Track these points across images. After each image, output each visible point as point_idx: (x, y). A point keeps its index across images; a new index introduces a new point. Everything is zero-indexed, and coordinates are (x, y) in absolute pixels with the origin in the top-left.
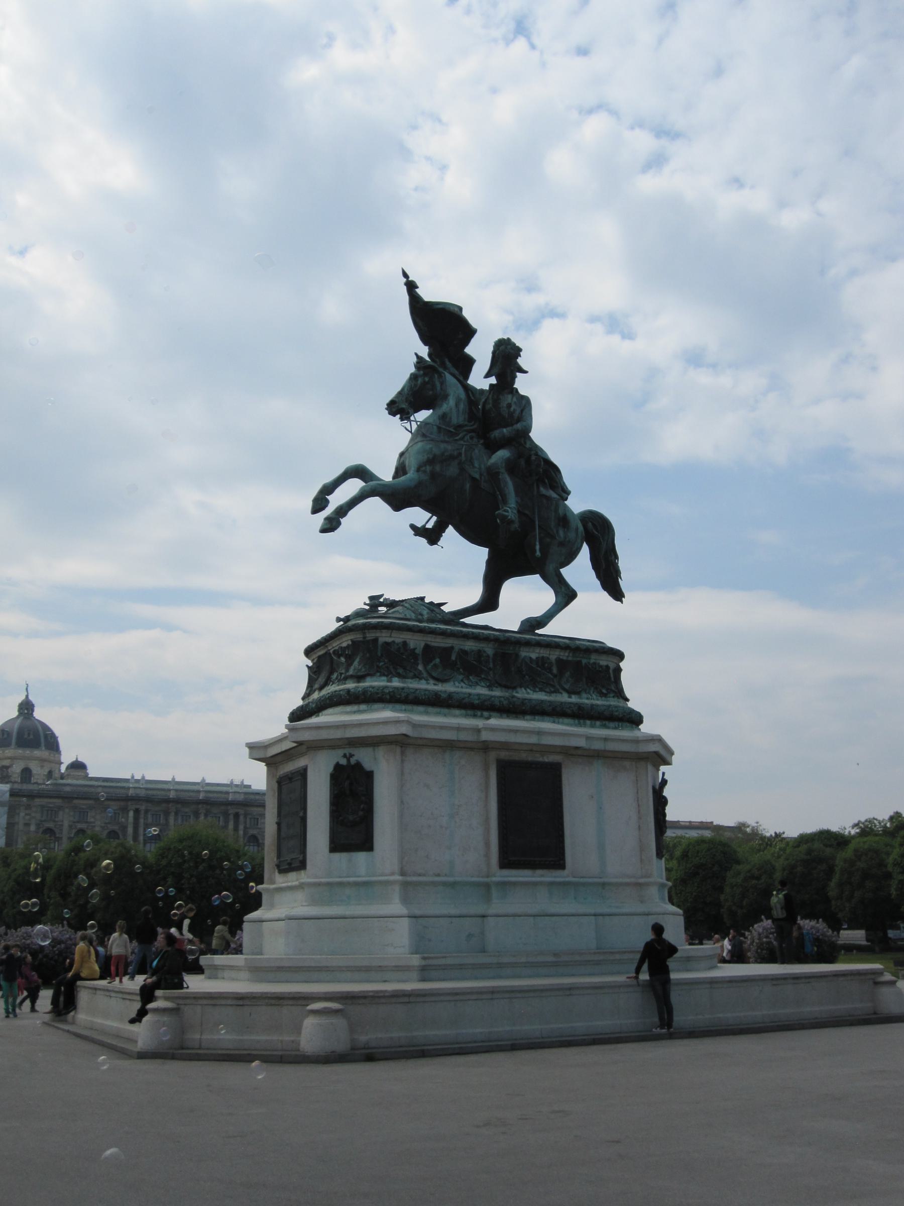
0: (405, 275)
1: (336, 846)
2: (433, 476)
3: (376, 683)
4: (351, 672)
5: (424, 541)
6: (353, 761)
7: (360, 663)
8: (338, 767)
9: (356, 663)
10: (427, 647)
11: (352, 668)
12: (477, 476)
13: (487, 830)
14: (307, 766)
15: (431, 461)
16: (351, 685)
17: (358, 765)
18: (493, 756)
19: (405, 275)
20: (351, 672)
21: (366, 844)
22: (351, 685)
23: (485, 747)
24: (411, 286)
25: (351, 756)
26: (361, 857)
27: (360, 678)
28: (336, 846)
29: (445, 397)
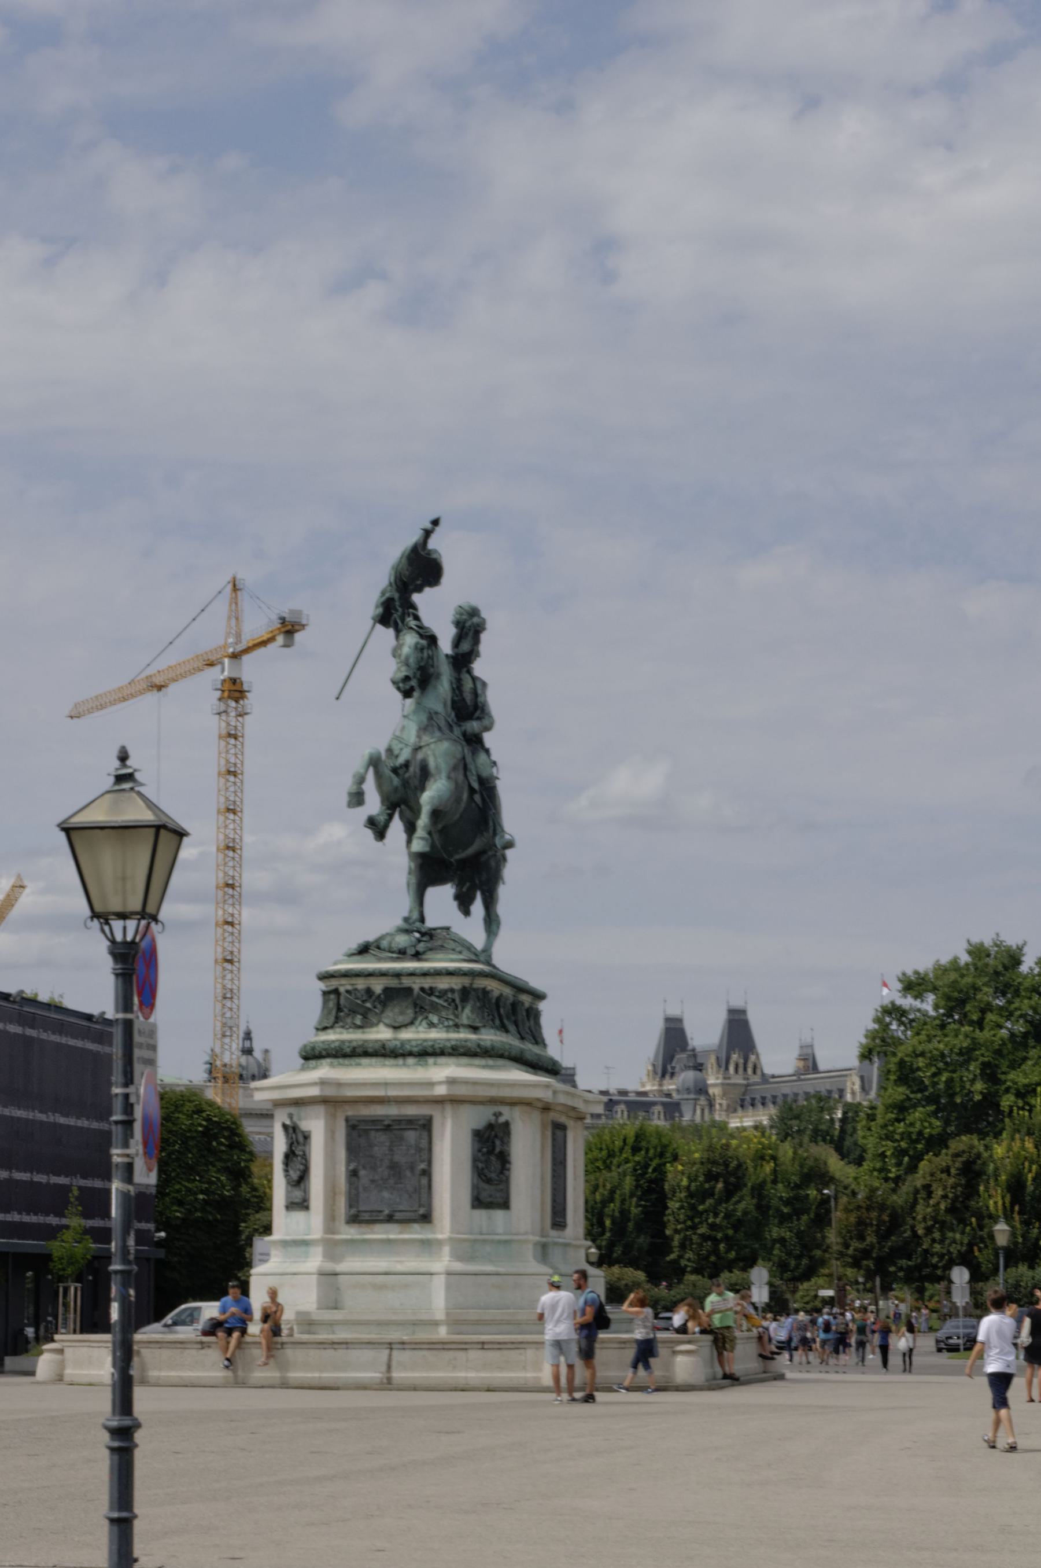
0: (436, 522)
1: (479, 1202)
2: (456, 783)
3: (489, 1037)
4: (464, 1020)
5: (369, 833)
6: (502, 1120)
7: (472, 1011)
8: (490, 1126)
9: (467, 1011)
10: (501, 995)
11: (464, 1016)
12: (476, 785)
13: (543, 1192)
15: (455, 768)
16: (464, 1035)
17: (507, 1124)
18: (552, 1115)
19: (436, 522)
20: (465, 1021)
21: (505, 1204)
22: (464, 1035)
23: (546, 1108)
24: (428, 533)
25: (500, 1114)
26: (499, 1214)
27: (475, 1029)
28: (479, 1202)
29: (438, 676)
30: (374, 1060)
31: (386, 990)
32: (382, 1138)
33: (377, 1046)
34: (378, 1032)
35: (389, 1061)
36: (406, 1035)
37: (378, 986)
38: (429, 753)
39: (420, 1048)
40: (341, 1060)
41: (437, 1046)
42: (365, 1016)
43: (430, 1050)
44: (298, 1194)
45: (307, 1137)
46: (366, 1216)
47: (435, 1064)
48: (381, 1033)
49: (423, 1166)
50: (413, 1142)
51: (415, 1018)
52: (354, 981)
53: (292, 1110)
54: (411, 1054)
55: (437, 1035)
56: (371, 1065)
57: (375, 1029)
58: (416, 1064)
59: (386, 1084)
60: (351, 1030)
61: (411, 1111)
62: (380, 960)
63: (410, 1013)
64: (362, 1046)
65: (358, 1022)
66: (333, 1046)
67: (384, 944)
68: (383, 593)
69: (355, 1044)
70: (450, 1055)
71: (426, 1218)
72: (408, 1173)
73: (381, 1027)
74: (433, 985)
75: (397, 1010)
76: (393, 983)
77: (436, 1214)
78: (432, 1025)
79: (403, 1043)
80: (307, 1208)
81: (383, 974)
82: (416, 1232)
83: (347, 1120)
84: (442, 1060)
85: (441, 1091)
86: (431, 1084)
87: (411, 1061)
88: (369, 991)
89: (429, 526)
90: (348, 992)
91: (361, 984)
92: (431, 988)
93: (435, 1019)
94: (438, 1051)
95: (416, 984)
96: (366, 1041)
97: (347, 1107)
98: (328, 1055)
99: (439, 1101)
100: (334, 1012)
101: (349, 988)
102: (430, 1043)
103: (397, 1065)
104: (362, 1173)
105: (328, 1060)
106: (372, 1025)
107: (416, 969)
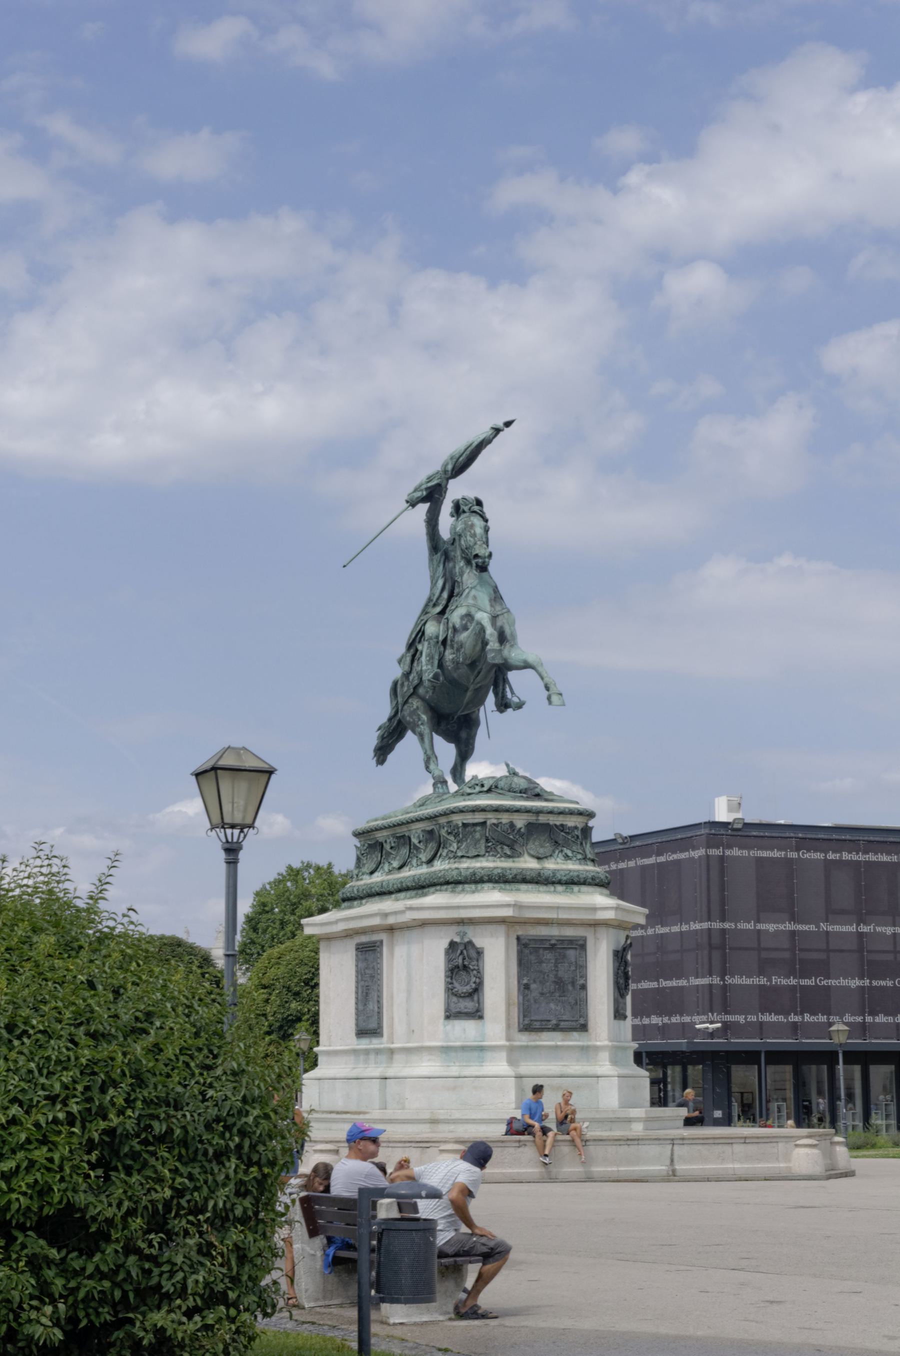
0: (508, 424)
14: (586, 938)
19: (508, 424)
24: (497, 431)
30: (530, 886)
31: (530, 826)
32: (548, 955)
33: (534, 874)
34: (525, 862)
35: (542, 888)
36: (551, 865)
37: (520, 822)
38: (505, 621)
39: (568, 877)
40: (502, 885)
41: (581, 876)
42: (511, 847)
43: (576, 880)
44: (468, 1005)
45: (480, 953)
46: (537, 1025)
47: (579, 892)
48: (528, 863)
49: (582, 982)
50: (573, 960)
51: (554, 852)
52: (500, 815)
53: (461, 928)
54: (560, 882)
55: (573, 867)
56: (527, 891)
57: (522, 859)
58: (564, 892)
59: (558, 908)
60: (503, 859)
61: (569, 932)
62: (514, 798)
63: (548, 848)
64: (521, 873)
65: (509, 853)
66: (495, 872)
67: (501, 784)
68: (430, 479)
69: (515, 872)
70: (590, 884)
71: (584, 1028)
72: (570, 988)
73: (526, 857)
74: (564, 823)
75: (537, 843)
76: (532, 818)
77: (591, 1024)
78: (567, 857)
79: (554, 872)
80: (481, 1017)
81: (528, 811)
82: (575, 1040)
83: (518, 938)
84: (584, 888)
85: (610, 915)
86: (594, 909)
87: (560, 888)
88: (512, 825)
89: (500, 424)
90: (494, 824)
91: (505, 818)
92: (562, 825)
93: (570, 853)
94: (582, 880)
95: (554, 820)
96: (523, 869)
97: (517, 927)
98: (490, 881)
99: (595, 925)
100: (483, 841)
101: (495, 821)
102: (576, 874)
103: (549, 892)
104: (533, 986)
105: (491, 885)
106: (520, 855)
107: (565, 808)
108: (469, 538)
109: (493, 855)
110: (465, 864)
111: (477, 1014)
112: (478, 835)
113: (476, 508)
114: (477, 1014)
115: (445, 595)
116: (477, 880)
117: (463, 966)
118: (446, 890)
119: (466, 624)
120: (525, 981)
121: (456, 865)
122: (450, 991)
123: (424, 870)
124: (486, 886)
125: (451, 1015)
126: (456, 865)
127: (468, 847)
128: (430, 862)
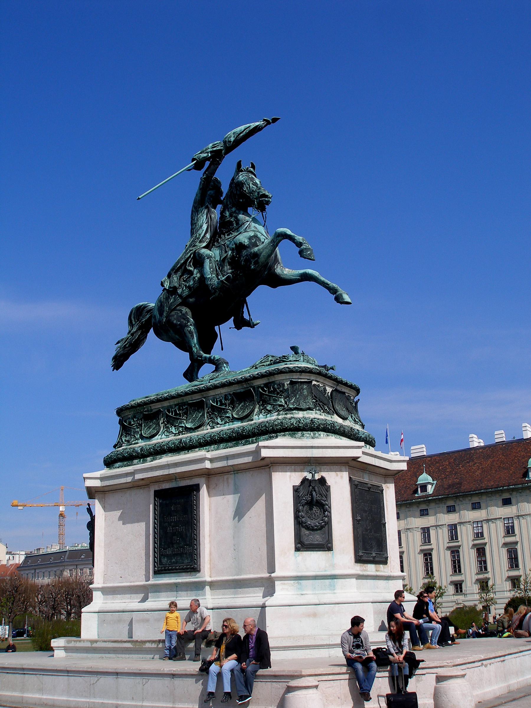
44: (317, 538)
100: (309, 398)
105: (325, 434)
108: (251, 185)
109: (319, 410)
110: (300, 415)
111: (326, 546)
112: (305, 392)
113: (252, 169)
114: (326, 546)
115: (208, 236)
116: (313, 427)
117: (311, 502)
118: (284, 435)
119: (255, 242)
120: (359, 518)
121: (289, 416)
122: (299, 523)
123: (237, 425)
124: (322, 433)
125: (301, 545)
126: (289, 416)
127: (297, 401)
128: (247, 417)
